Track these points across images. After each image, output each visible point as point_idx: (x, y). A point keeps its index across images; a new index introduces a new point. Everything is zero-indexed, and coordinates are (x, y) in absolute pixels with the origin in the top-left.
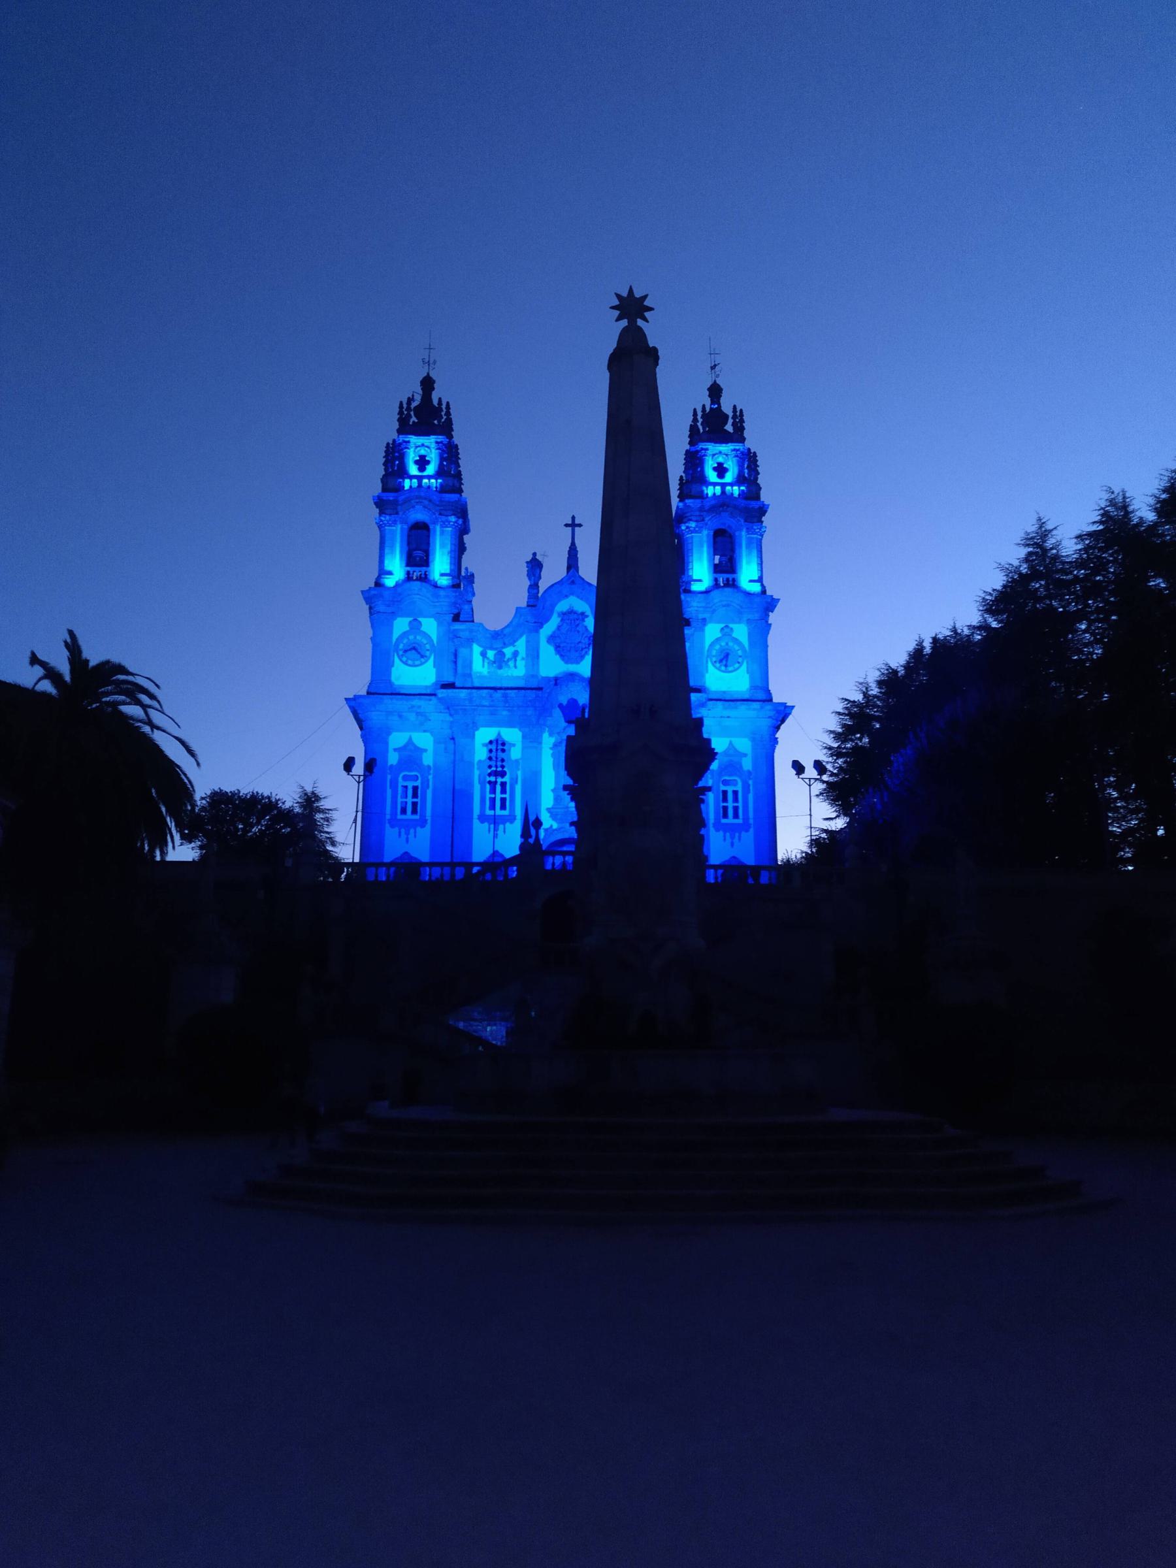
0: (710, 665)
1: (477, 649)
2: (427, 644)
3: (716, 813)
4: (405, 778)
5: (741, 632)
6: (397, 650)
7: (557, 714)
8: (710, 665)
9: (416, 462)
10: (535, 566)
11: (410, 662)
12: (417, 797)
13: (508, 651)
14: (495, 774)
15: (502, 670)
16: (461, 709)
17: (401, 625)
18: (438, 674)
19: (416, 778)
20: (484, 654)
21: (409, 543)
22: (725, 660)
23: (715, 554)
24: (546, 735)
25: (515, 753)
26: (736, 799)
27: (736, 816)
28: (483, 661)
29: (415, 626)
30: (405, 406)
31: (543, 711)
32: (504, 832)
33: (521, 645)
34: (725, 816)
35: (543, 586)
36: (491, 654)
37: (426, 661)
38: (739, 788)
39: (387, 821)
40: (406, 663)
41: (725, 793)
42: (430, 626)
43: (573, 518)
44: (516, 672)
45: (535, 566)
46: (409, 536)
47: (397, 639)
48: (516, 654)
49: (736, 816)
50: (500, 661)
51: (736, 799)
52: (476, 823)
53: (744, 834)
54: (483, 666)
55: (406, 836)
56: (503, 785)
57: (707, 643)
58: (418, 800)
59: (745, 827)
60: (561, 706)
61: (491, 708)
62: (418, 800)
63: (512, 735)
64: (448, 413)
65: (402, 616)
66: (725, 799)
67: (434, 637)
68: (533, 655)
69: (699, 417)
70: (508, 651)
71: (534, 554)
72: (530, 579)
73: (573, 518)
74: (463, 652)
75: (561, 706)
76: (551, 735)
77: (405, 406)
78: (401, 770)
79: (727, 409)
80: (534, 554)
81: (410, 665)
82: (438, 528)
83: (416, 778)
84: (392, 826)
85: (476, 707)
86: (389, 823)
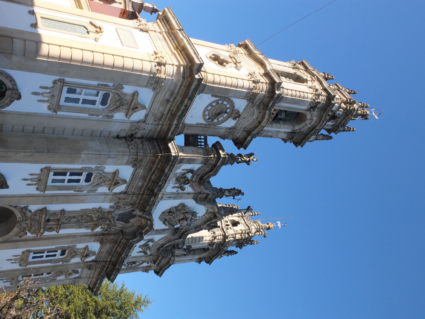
2: (218, 120)
11: (210, 108)
12: (82, 103)
15: (175, 180)
16: (155, 161)
20: (191, 171)
28: (187, 170)
32: (29, 185)
36: (189, 176)
37: (204, 119)
39: (62, 78)
40: (210, 104)
47: (232, 101)
54: (183, 170)
55: (41, 92)
61: (148, 178)
65: (248, 105)
71: (243, 194)
76: (111, 207)
81: (207, 107)
82: (289, 130)
84: (55, 82)
85: (152, 171)
86: (59, 80)
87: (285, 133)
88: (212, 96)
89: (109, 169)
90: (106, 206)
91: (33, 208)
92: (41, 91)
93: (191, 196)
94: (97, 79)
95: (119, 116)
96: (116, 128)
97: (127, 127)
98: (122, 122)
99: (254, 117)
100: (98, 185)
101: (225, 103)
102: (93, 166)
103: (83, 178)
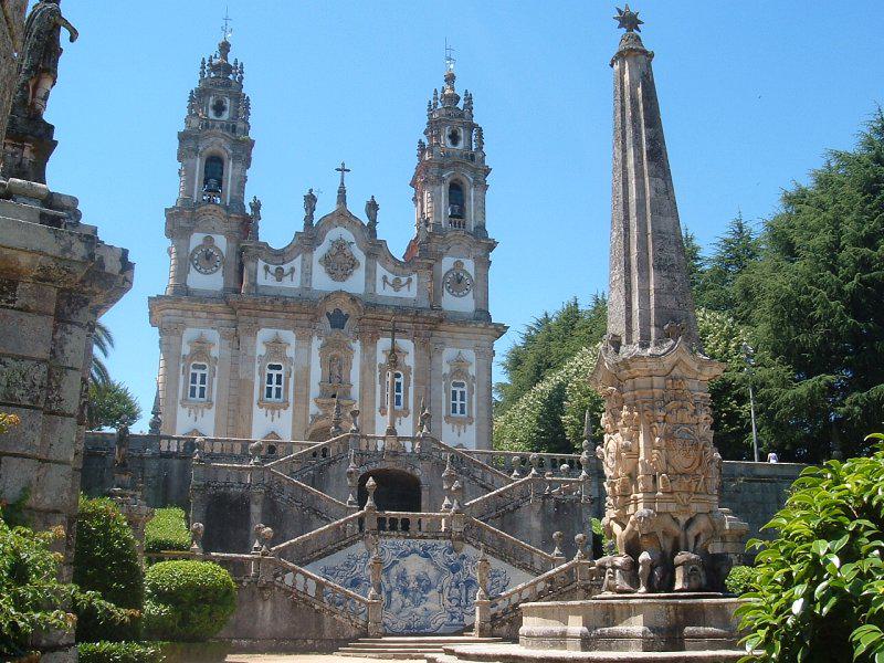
0: (445, 291)
1: (261, 264)
3: (447, 409)
4: (195, 367)
5: (469, 266)
6: (192, 260)
7: (325, 320)
8: (445, 291)
9: (214, 108)
10: (311, 200)
11: (203, 270)
13: (286, 268)
14: (271, 367)
17: (197, 239)
18: (226, 283)
19: (204, 367)
20: (267, 269)
21: (206, 172)
22: (458, 282)
23: (450, 203)
24: (315, 338)
25: (290, 352)
26: (462, 399)
27: (462, 412)
29: (209, 240)
30: (207, 62)
31: (315, 319)
33: (297, 263)
34: (454, 411)
35: (317, 216)
36: (273, 268)
38: (465, 389)
41: (454, 393)
42: (221, 242)
43: (343, 164)
44: (292, 284)
45: (311, 200)
46: (206, 167)
48: (293, 270)
49: (462, 412)
50: (280, 275)
51: (462, 399)
52: (256, 407)
53: (468, 427)
56: (279, 376)
57: (443, 273)
58: (190, 385)
59: (470, 420)
60: (328, 314)
62: (190, 385)
63: (289, 336)
64: (241, 72)
66: (454, 398)
67: (224, 250)
68: (307, 273)
69: (439, 96)
70: (286, 268)
71: (311, 190)
72: (306, 210)
73: (343, 164)
74: (249, 266)
75: (328, 314)
76: (319, 338)
77: (207, 62)
78: (191, 359)
79: (460, 92)
80: (311, 190)
83: (204, 367)
84: (184, 406)
87: (234, 168)
88: (188, 272)
89: (261, 350)
90: (316, 343)
91: (313, 409)
92: (193, 415)
93: (308, 257)
94: (178, 376)
95: (215, 352)
96: (228, 353)
97: (226, 342)
98: (221, 348)
99: (210, 217)
100: (284, 359)
101: (196, 256)
102: (257, 365)
103: (275, 373)
